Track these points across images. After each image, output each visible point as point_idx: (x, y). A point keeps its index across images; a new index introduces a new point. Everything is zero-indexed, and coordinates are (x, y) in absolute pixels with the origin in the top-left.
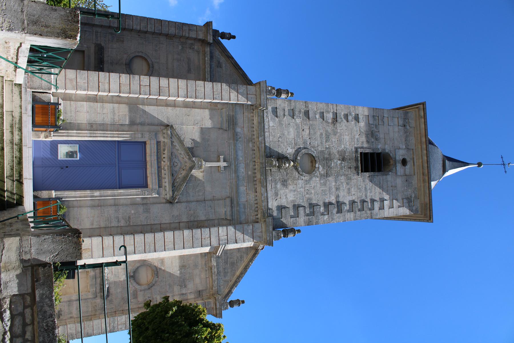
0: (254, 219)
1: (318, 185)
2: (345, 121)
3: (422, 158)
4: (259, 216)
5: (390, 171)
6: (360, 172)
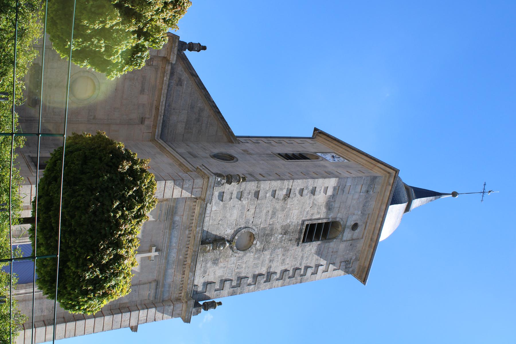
0: (177, 296)
1: (252, 260)
2: (298, 195)
3: (376, 224)
4: (183, 294)
5: (334, 238)
6: (301, 242)
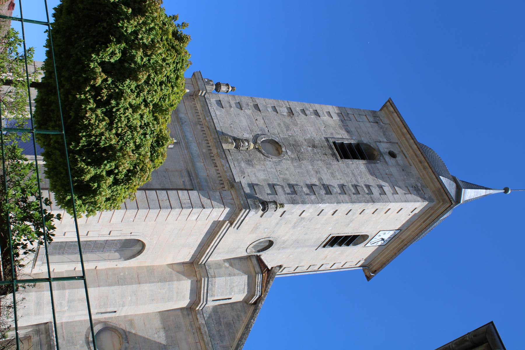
6: (339, 158)
